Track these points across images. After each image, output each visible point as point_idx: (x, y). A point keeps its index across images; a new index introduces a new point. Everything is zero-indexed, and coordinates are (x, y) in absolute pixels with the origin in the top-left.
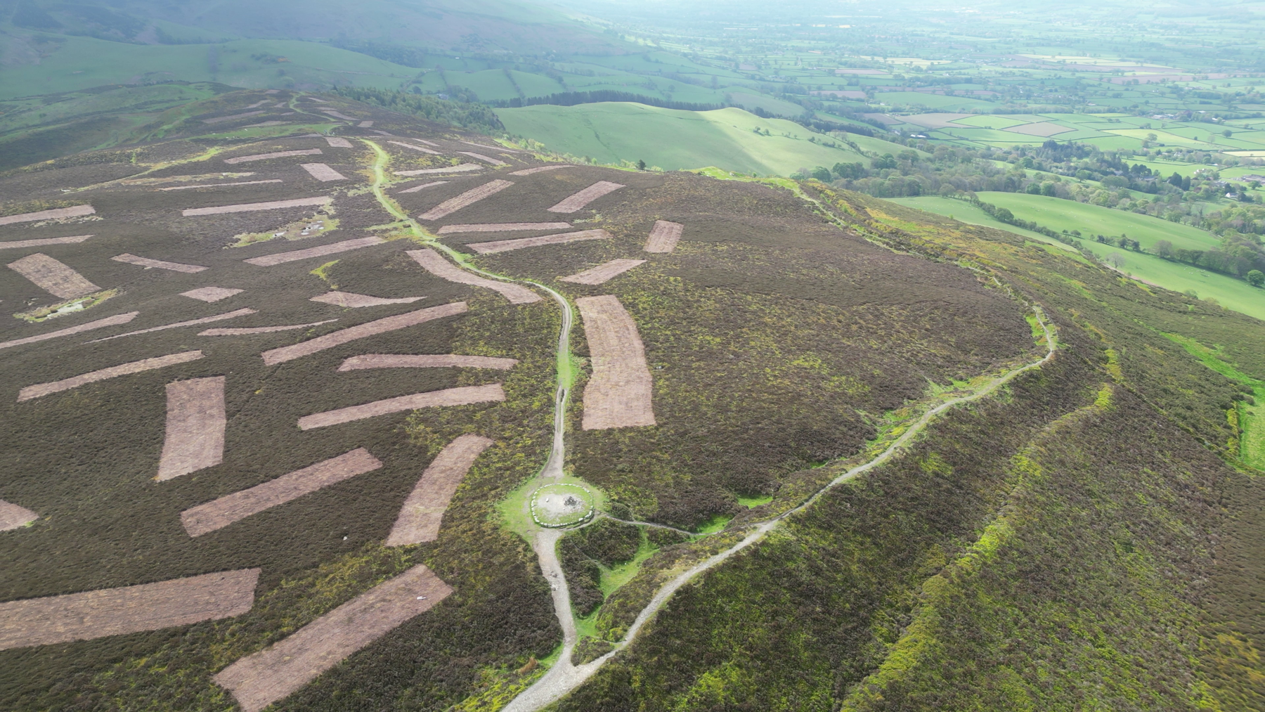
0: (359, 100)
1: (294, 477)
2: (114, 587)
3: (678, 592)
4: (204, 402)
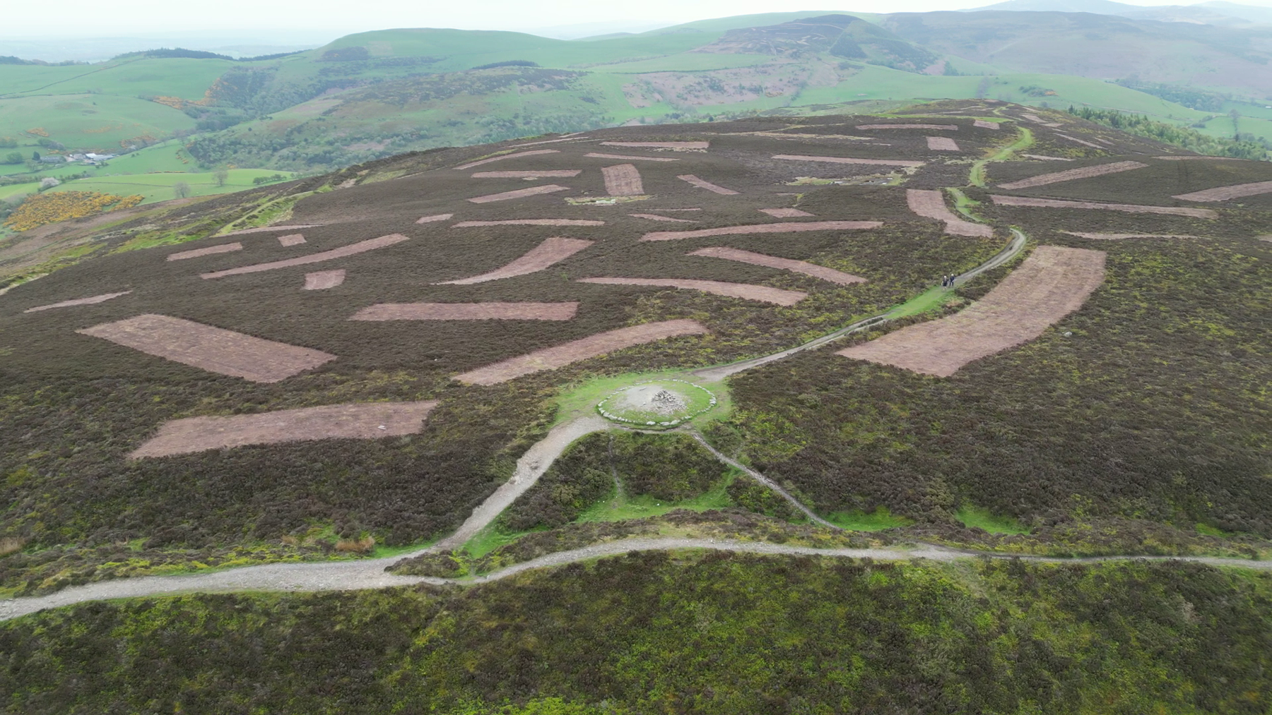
0: (1088, 119)
3: (634, 555)
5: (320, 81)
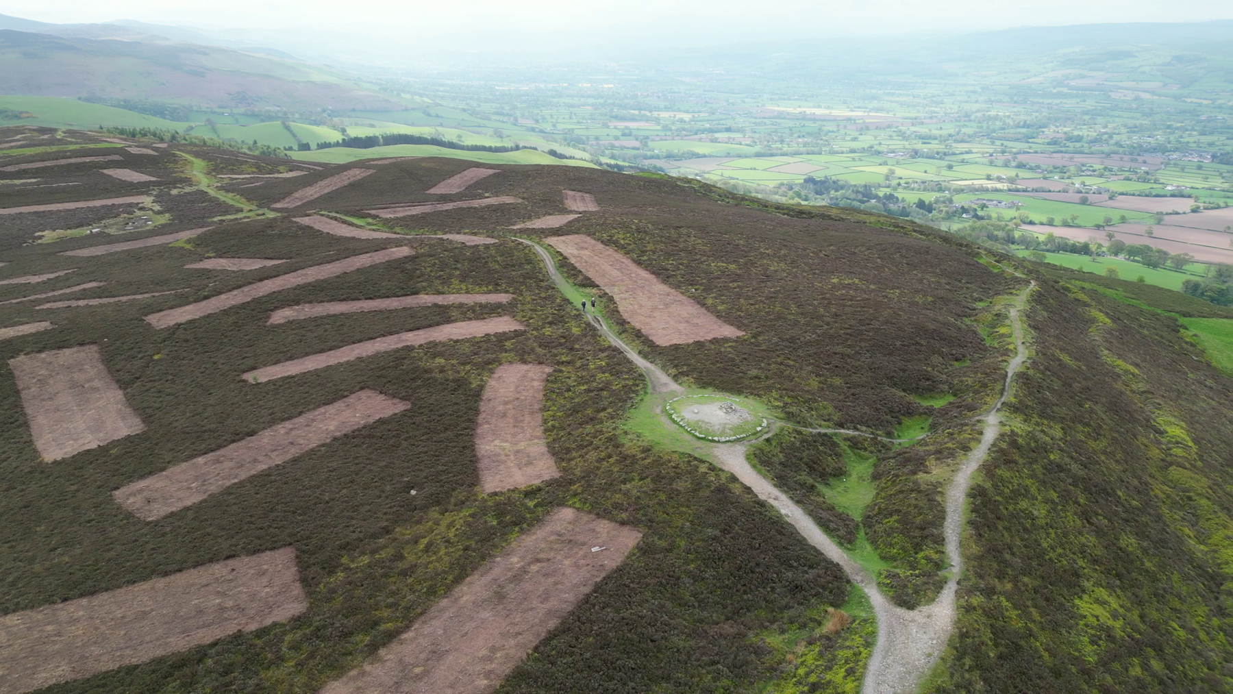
1: (282, 431)
2: (32, 607)
4: (75, 376)
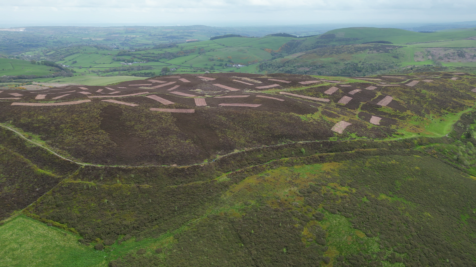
5: (315, 46)
